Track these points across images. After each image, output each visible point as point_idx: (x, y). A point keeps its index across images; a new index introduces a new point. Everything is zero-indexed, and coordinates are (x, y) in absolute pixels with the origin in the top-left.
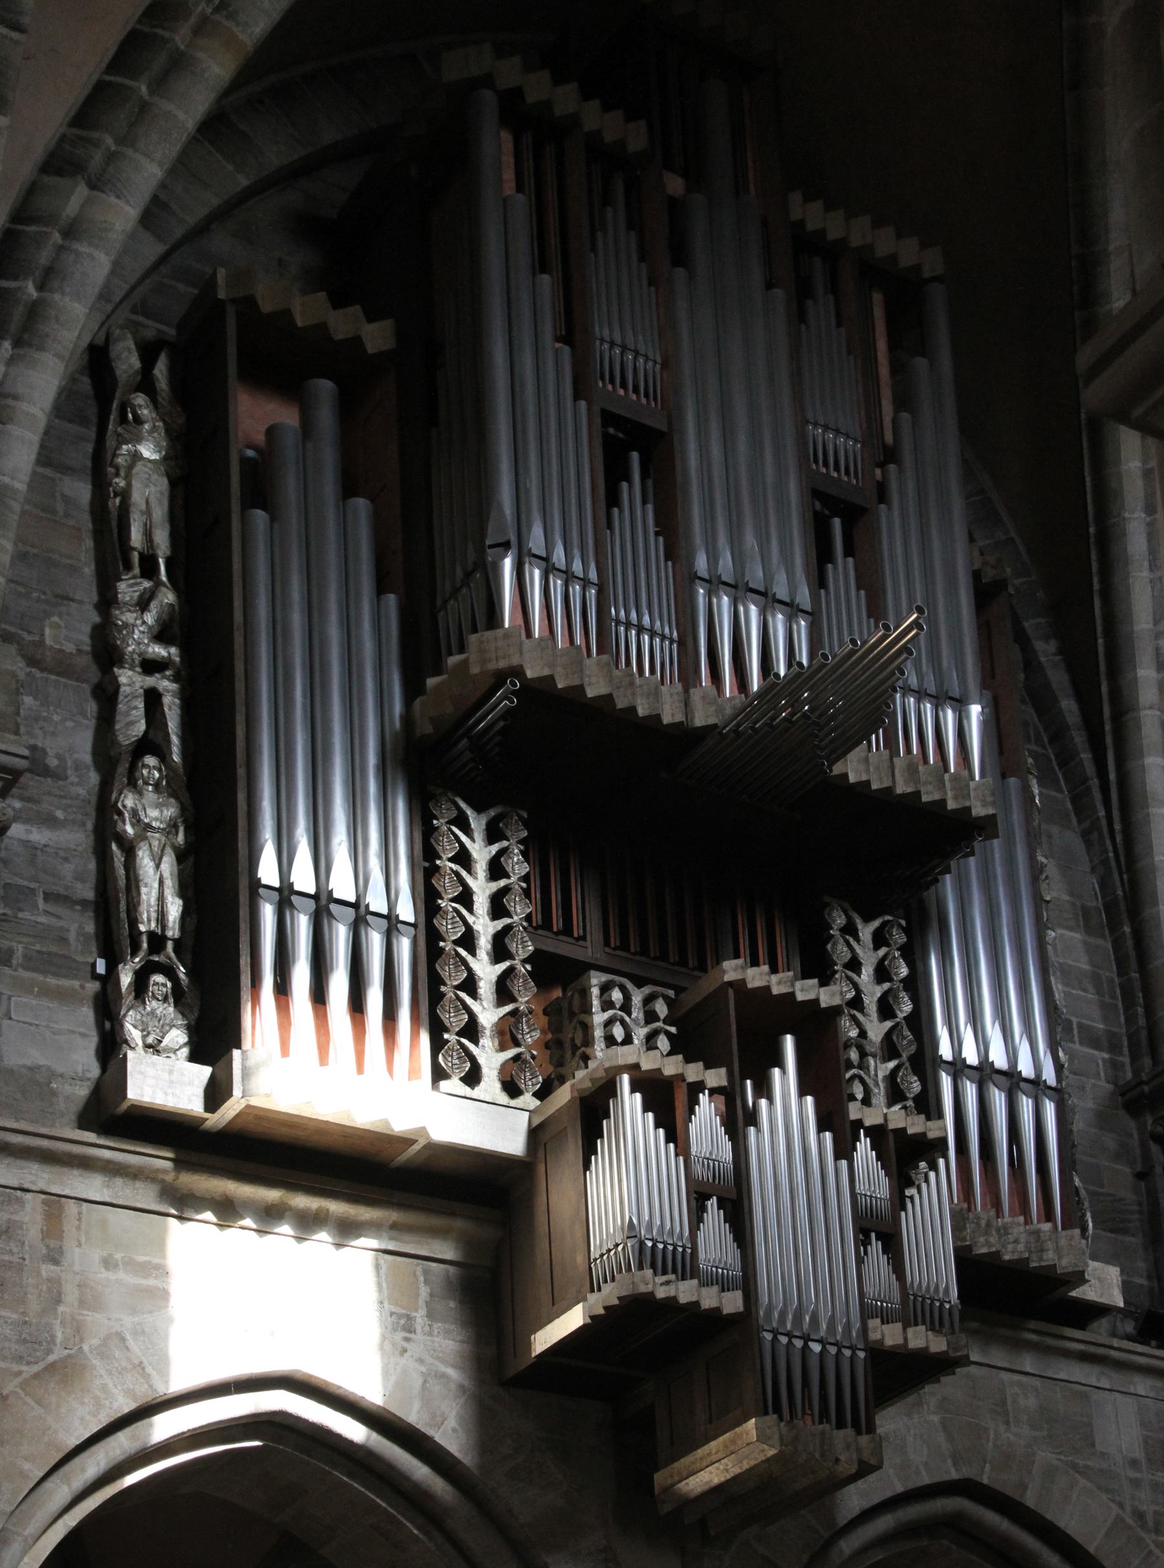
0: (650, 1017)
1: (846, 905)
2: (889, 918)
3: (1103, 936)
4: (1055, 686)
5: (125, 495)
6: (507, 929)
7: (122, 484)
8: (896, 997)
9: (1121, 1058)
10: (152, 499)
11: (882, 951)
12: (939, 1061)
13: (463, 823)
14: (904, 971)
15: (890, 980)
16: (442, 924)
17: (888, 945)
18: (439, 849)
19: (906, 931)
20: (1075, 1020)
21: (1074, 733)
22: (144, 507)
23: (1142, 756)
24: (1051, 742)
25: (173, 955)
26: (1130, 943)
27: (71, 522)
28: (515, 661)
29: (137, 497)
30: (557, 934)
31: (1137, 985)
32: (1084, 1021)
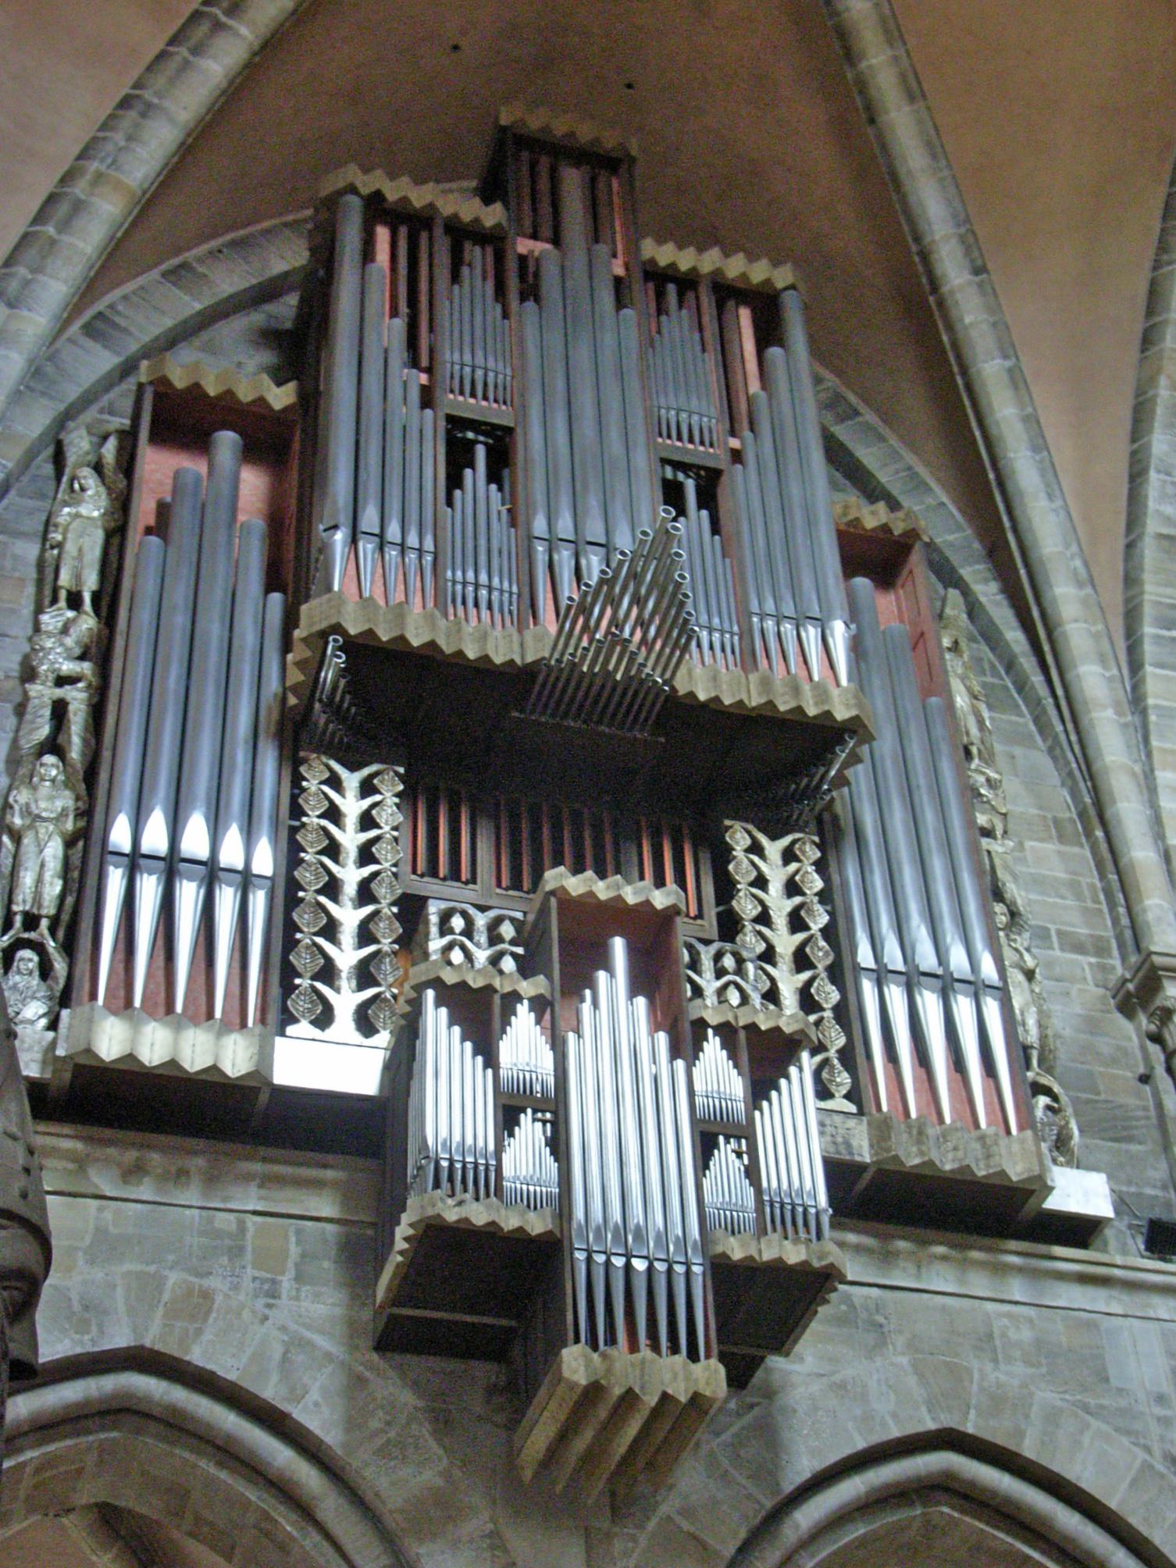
0: (494, 939)
1: (750, 827)
2: (798, 835)
3: (1082, 846)
4: (998, 621)
5: (60, 545)
6: (375, 875)
7: (59, 537)
8: (810, 911)
9: (1111, 961)
10: (86, 549)
11: (794, 866)
12: (857, 969)
13: (335, 782)
14: (819, 884)
15: (803, 894)
16: (303, 875)
17: (798, 860)
18: (306, 808)
19: (821, 846)
20: (1052, 928)
21: (1022, 660)
22: (75, 553)
23: (1075, 667)
24: (1007, 673)
25: (46, 932)
26: (1104, 847)
27: (17, 574)
28: (334, 621)
29: (70, 548)
30: (444, 879)
31: (1116, 886)
32: (1063, 928)
